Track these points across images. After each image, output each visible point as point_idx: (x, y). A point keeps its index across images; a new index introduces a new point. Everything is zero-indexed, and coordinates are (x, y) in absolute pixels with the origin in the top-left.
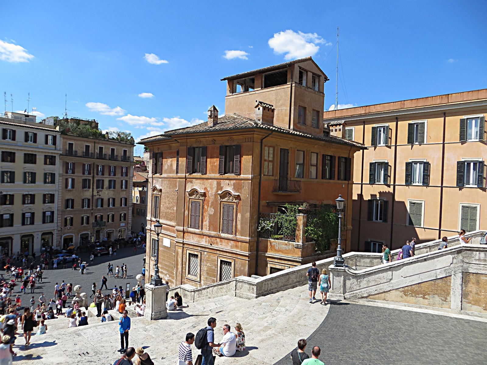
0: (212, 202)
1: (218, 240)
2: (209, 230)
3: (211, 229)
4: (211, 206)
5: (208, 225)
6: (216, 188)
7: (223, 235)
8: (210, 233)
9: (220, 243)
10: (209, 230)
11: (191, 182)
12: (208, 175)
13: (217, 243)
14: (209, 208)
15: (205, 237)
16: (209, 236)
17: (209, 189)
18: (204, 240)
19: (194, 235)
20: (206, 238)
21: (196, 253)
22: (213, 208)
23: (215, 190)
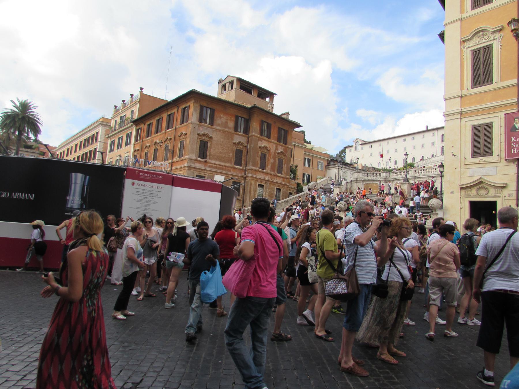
1: (275, 177)
2: (271, 171)
4: (272, 158)
7: (279, 175)
10: (271, 171)
11: (261, 141)
12: (271, 140)
13: (274, 179)
16: (271, 175)
17: (271, 148)
21: (263, 184)
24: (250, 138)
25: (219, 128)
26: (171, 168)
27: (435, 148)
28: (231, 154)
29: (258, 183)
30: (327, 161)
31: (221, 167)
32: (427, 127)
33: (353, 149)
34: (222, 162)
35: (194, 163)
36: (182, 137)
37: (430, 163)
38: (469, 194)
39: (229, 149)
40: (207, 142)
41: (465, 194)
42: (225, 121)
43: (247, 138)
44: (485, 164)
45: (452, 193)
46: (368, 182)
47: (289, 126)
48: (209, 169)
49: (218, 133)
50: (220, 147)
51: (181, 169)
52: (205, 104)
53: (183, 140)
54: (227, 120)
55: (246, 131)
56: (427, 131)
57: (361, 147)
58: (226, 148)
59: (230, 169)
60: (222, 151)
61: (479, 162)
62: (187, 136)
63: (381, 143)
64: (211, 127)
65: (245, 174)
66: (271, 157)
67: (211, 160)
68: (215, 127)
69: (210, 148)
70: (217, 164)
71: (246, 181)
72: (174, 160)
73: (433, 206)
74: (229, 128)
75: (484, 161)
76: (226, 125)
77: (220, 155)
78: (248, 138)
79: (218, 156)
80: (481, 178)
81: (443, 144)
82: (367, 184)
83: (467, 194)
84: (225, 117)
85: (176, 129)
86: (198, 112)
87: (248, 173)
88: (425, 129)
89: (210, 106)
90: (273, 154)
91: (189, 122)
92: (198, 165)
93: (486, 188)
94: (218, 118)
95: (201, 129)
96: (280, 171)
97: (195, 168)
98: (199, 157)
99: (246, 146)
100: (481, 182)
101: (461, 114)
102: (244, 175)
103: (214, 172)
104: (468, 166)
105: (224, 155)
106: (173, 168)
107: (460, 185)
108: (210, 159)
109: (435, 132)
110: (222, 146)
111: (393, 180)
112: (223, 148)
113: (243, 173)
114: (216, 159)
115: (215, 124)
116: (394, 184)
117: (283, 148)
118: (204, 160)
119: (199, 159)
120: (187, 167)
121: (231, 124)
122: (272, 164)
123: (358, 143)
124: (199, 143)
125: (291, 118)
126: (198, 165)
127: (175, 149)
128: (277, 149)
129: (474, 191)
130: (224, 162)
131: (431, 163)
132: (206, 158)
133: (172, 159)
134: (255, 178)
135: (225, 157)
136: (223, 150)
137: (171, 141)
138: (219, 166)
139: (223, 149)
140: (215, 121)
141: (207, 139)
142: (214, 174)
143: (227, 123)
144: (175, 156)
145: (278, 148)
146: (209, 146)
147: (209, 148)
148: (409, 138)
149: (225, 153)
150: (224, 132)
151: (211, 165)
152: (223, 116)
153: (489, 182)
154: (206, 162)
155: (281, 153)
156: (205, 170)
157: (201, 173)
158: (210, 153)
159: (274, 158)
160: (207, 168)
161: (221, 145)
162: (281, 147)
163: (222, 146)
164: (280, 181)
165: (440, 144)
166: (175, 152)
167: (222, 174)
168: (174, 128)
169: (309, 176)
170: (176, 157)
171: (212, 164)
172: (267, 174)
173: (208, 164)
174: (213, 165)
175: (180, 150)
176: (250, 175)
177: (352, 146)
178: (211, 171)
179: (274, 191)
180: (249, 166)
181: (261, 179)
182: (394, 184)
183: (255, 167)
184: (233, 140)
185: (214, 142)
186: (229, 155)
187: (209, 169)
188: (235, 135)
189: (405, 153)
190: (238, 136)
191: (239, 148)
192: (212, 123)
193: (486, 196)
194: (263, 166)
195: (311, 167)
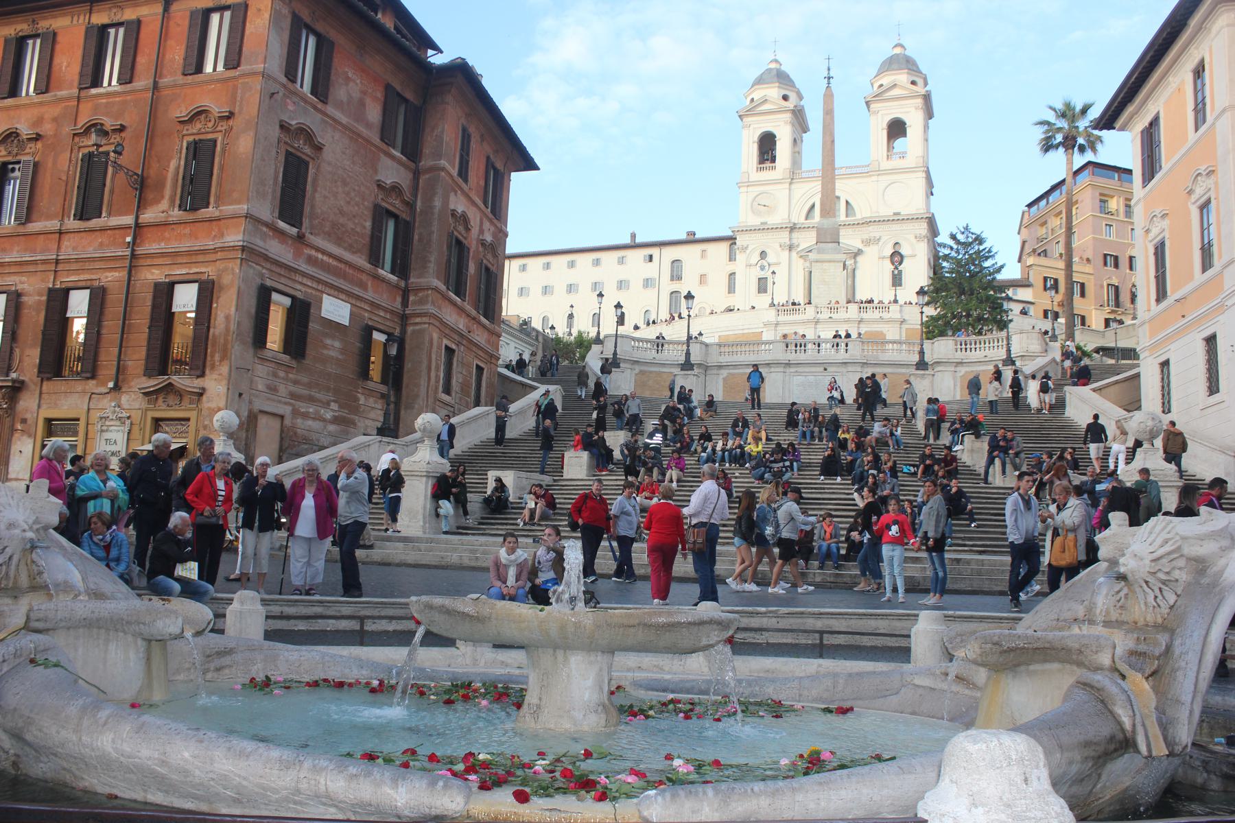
21: (454, 347)
24: (423, 179)
25: (344, 120)
26: (133, 250)
27: (652, 293)
29: (445, 342)
31: (342, 266)
32: (633, 236)
34: (345, 249)
35: (264, 237)
36: (197, 126)
40: (307, 164)
43: (410, 176)
48: (310, 270)
49: (337, 135)
50: (340, 190)
51: (201, 258)
52: (305, 15)
53: (210, 136)
55: (412, 151)
58: (357, 199)
59: (364, 277)
62: (236, 123)
64: (320, 106)
65: (405, 303)
67: (316, 235)
68: (330, 109)
69: (315, 190)
70: (330, 255)
71: (410, 329)
74: (368, 126)
77: (341, 220)
82: (642, 372)
84: (358, 81)
86: (286, 36)
87: (422, 302)
89: (319, 27)
91: (244, 68)
92: (275, 248)
97: (266, 258)
98: (282, 217)
103: (326, 284)
105: (351, 225)
106: (140, 250)
109: (655, 252)
110: (347, 189)
114: (328, 235)
115: (330, 98)
116: (721, 377)
118: (294, 231)
119: (282, 225)
120: (243, 248)
121: (374, 113)
124: (282, 158)
126: (275, 248)
128: (481, 231)
135: (352, 229)
136: (349, 203)
137: (123, 135)
138: (335, 263)
141: (307, 150)
142: (323, 292)
143: (362, 104)
144: (157, 201)
146: (309, 179)
147: (309, 187)
149: (354, 216)
150: (355, 136)
151: (313, 252)
152: (354, 77)
154: (300, 237)
156: (296, 271)
157: (283, 280)
158: (313, 207)
160: (304, 267)
161: (345, 183)
163: (347, 189)
165: (667, 286)
167: (343, 297)
170: (164, 204)
171: (318, 250)
172: (461, 310)
173: (307, 251)
174: (320, 256)
176: (430, 308)
178: (312, 278)
179: (471, 373)
182: (721, 377)
184: (376, 171)
187: (310, 270)
190: (389, 162)
191: (391, 204)
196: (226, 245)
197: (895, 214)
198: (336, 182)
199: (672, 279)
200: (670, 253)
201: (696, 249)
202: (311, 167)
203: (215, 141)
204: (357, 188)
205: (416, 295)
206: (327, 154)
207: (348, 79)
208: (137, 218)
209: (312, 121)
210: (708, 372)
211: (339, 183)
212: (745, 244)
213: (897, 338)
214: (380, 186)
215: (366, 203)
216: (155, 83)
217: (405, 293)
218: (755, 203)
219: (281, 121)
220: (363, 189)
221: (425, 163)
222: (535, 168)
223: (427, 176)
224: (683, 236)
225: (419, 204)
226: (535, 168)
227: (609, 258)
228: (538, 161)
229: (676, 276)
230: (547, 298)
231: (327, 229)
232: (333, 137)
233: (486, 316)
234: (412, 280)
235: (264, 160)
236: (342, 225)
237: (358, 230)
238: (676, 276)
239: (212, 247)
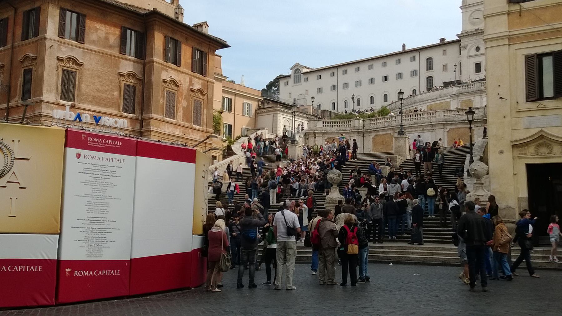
0: (186, 96)
1: (190, 131)
2: (183, 121)
3: (185, 120)
5: (182, 116)
6: (188, 83)
7: (196, 127)
8: (184, 124)
9: (191, 134)
10: (183, 121)
11: (167, 71)
13: (189, 134)
14: (183, 100)
15: (179, 127)
18: (178, 130)
19: (169, 124)
20: (180, 128)
22: (186, 101)
23: (187, 84)
24: (147, 66)
25: (96, 48)
27: (416, 79)
28: (116, 93)
30: (258, 101)
32: (404, 46)
33: (291, 81)
34: (102, 107)
36: (26, 63)
37: (415, 103)
38: (525, 154)
39: (113, 84)
40: (75, 73)
41: (520, 154)
42: (104, 35)
43: (141, 66)
44: (545, 111)
45: (501, 152)
46: (331, 136)
47: (209, 45)
49: (92, 57)
50: (97, 81)
53: (31, 67)
54: (108, 33)
56: (404, 52)
57: (303, 77)
58: (108, 83)
60: (100, 89)
61: (537, 107)
63: (335, 71)
64: (80, 45)
65: (141, 126)
66: (182, 98)
67: (83, 103)
68: (86, 45)
72: (12, 104)
73: (476, 173)
74: (111, 47)
75: (544, 106)
76: (105, 42)
77: (98, 94)
78: (144, 65)
79: (94, 97)
80: (541, 131)
81: (429, 73)
83: (522, 154)
84: (104, 29)
85: (13, 48)
88: (400, 49)
89: (77, 10)
90: (185, 92)
93: (548, 146)
94: (92, 31)
95: (63, 49)
96: (197, 121)
98: (62, 98)
99: (140, 80)
100: (542, 137)
101: (509, 39)
102: (139, 128)
104: (522, 114)
105: (104, 95)
107: (512, 142)
108: (81, 101)
109: (417, 55)
111: (370, 132)
112: (101, 82)
113: (138, 125)
114: (91, 102)
115: (86, 39)
116: (371, 137)
117: (201, 82)
122: (184, 108)
123: (298, 71)
124: (61, 73)
125: (212, 31)
127: (13, 84)
128: (191, 83)
129: (531, 150)
130: (105, 106)
131: (417, 103)
132: (74, 100)
133: (9, 102)
134: (159, 133)
135: (105, 97)
136: (102, 86)
139: (102, 84)
140: (86, 36)
141: (76, 67)
143: (107, 39)
144: (15, 97)
145: (193, 82)
146: (77, 79)
148: (377, 65)
149: (106, 91)
152: (101, 27)
153: (553, 136)
155: (200, 91)
159: (187, 98)
161: (99, 77)
162: (197, 80)
164: (198, 138)
165: (424, 74)
166: (12, 89)
168: (9, 46)
169: (230, 126)
170: (17, 98)
172: (177, 125)
175: (24, 86)
177: (289, 76)
180: (147, 113)
181: (168, 135)
182: (371, 137)
183: (158, 114)
184: (119, 68)
185: (86, 73)
186: (113, 95)
188: (122, 60)
189: (399, 91)
190: (126, 62)
192: (80, 37)
193: (549, 156)
194: (171, 113)
195: (233, 112)
196: (35, 114)
197: (280, 75)
198: (94, 78)
199: (427, 70)
200: (425, 55)
201: (440, 51)
202: (78, 73)
203: (32, 69)
204: (107, 78)
205: (145, 122)
206: (87, 65)
207: (97, 30)
208: (8, 105)
209: (77, 54)
210: (365, 135)
211: (96, 78)
212: (466, 44)
213: (400, 116)
214: (121, 75)
215: (113, 84)
216: (13, 45)
217: (141, 121)
218: (472, 18)
219: (58, 57)
220: (110, 78)
221: (148, 59)
222: (230, 47)
223: (148, 66)
224: (438, 42)
225: (145, 79)
226: (227, 46)
227: (391, 62)
228: (228, 43)
229: (430, 67)
230: (372, 85)
231: (90, 100)
232: (90, 58)
233: (197, 124)
234: (144, 115)
235: (49, 76)
236: (99, 96)
237: (109, 97)
238: (430, 67)
239: (31, 116)
